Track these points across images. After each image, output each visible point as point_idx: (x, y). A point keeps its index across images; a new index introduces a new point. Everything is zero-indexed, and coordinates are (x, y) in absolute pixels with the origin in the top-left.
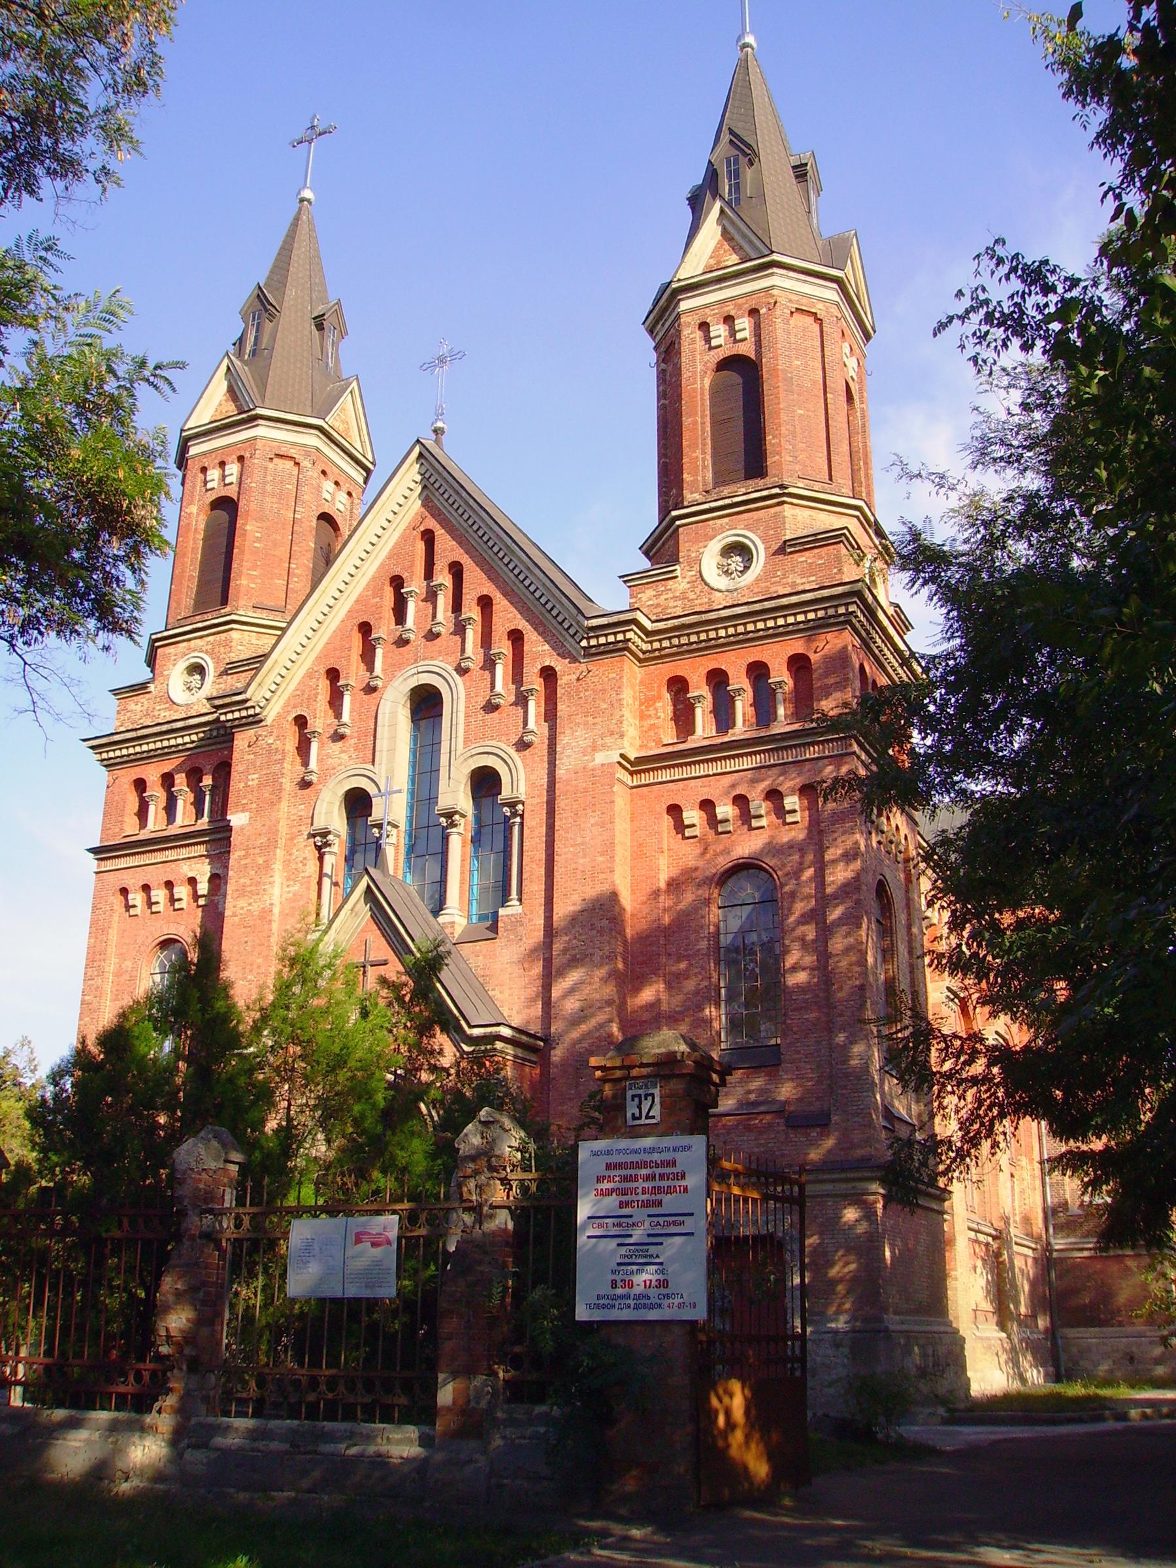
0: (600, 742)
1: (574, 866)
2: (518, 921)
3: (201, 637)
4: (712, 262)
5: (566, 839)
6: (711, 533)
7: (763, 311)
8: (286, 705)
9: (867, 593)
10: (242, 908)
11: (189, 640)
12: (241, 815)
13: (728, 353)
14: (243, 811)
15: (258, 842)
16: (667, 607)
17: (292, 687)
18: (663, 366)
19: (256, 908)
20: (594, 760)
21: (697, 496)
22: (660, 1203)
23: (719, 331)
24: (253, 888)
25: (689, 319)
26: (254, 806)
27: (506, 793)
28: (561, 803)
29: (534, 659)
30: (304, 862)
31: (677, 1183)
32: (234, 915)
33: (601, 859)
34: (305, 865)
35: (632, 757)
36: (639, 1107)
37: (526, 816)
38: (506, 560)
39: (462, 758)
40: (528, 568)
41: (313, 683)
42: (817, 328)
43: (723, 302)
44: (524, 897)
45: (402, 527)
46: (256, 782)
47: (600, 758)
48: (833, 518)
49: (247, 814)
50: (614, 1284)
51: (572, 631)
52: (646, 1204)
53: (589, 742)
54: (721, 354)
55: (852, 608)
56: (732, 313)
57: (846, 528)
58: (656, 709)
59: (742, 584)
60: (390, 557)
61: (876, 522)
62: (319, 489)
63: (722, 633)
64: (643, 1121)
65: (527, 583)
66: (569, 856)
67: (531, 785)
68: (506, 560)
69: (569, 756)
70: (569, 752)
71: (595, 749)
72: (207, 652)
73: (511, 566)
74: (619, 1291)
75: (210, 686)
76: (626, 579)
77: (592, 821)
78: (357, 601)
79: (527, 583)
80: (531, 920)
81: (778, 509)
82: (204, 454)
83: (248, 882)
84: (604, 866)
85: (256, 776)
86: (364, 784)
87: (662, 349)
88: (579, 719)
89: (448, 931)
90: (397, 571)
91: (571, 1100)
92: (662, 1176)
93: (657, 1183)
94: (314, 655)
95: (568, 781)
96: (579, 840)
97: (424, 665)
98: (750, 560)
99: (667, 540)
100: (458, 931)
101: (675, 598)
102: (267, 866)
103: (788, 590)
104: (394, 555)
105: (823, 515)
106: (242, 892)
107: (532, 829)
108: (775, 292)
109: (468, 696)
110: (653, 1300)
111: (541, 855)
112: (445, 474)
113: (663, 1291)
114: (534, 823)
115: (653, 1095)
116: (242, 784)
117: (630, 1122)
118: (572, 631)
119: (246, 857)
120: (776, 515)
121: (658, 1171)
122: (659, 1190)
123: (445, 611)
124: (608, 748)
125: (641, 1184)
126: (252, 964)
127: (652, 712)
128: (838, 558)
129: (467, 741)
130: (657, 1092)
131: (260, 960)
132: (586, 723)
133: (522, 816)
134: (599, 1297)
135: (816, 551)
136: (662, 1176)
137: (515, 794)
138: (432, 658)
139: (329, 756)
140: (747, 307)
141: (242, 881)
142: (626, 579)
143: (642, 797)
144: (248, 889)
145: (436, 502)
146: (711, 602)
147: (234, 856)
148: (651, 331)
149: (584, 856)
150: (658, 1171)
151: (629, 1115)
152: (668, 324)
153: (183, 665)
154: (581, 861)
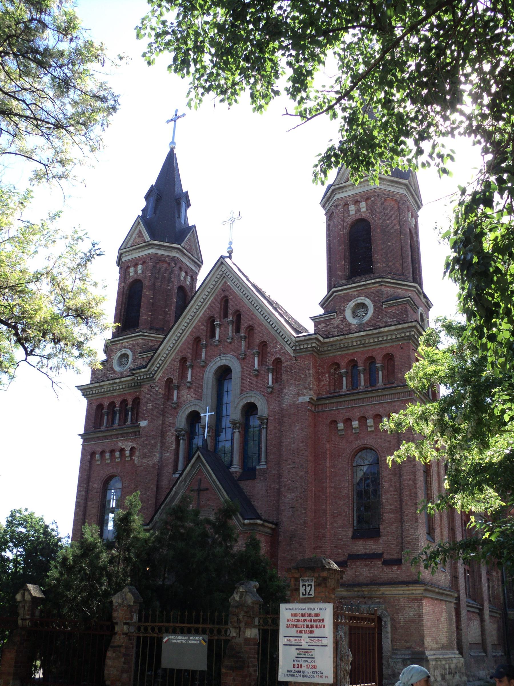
2: (264, 471)
3: (127, 342)
6: (350, 298)
8: (162, 374)
9: (419, 327)
11: (122, 343)
13: (357, 218)
14: (145, 420)
16: (330, 332)
17: (166, 366)
18: (329, 222)
19: (150, 463)
21: (344, 281)
22: (313, 632)
27: (259, 413)
29: (272, 355)
31: (320, 623)
33: (301, 445)
35: (315, 399)
36: (305, 590)
38: (260, 310)
41: (175, 363)
42: (396, 206)
43: (354, 195)
45: (214, 295)
47: (301, 399)
48: (404, 292)
50: (294, 666)
51: (288, 343)
52: (308, 632)
53: (296, 392)
54: (355, 218)
55: (413, 333)
56: (359, 200)
57: (409, 297)
59: (364, 322)
60: (208, 308)
61: (423, 293)
62: (179, 275)
63: (355, 344)
64: (307, 596)
65: (269, 321)
68: (260, 310)
70: (287, 396)
71: (298, 395)
72: (129, 348)
73: (262, 313)
74: (296, 669)
75: (130, 364)
76: (313, 319)
78: (194, 327)
79: (269, 321)
80: (270, 471)
81: (379, 288)
82: (129, 261)
86: (197, 409)
87: (329, 215)
89: (234, 475)
92: (314, 621)
93: (312, 623)
94: (176, 351)
96: (292, 436)
97: (224, 357)
98: (367, 310)
99: (331, 301)
100: (238, 475)
101: (334, 328)
102: (156, 443)
103: (384, 324)
104: (211, 307)
108: (377, 190)
109: (243, 371)
110: (311, 674)
113: (314, 670)
114: (272, 428)
115: (311, 585)
117: (301, 596)
118: (288, 343)
119: (146, 440)
120: (378, 291)
121: (313, 618)
122: (313, 626)
123: (232, 333)
124: (305, 395)
125: (306, 623)
127: (324, 379)
128: (407, 311)
129: (242, 391)
130: (313, 584)
133: (267, 424)
134: (288, 671)
135: (396, 307)
136: (314, 621)
138: (227, 354)
139: (182, 396)
142: (313, 319)
146: (350, 329)
148: (324, 206)
149: (294, 443)
150: (313, 618)
151: (301, 594)
152: (331, 204)
153: (119, 354)
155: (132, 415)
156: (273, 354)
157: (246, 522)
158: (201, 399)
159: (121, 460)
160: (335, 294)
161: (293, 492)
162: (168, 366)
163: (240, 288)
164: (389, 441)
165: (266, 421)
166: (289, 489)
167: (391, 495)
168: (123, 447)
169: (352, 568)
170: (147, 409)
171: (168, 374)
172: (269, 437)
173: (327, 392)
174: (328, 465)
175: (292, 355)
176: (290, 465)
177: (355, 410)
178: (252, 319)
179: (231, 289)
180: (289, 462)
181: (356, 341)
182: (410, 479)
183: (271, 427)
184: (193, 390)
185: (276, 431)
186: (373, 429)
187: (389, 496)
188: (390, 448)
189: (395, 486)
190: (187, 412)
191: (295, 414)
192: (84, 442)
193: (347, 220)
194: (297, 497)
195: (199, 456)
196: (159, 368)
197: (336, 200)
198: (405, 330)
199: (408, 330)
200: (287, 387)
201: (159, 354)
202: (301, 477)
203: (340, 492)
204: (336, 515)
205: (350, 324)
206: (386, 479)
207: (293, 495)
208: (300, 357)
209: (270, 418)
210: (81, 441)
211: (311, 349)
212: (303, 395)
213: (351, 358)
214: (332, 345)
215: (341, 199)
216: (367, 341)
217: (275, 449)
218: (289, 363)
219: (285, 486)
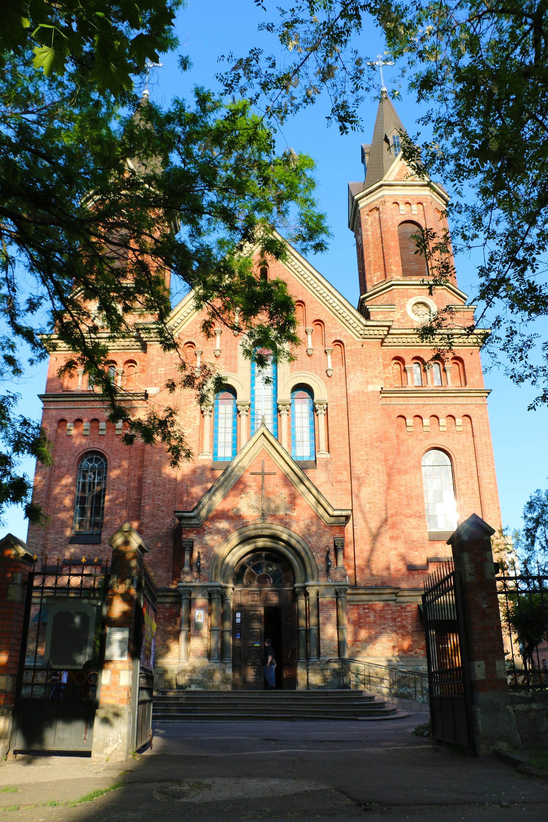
0: (370, 380)
4: (398, 177)
5: (355, 424)
7: (425, 204)
14: (155, 386)
21: (399, 277)
23: (402, 207)
28: (352, 406)
30: (194, 418)
39: (290, 378)
46: (163, 372)
47: (371, 388)
66: (358, 433)
67: (332, 396)
70: (353, 382)
71: (367, 383)
85: (163, 369)
88: (358, 368)
96: (363, 425)
105: (455, 299)
107: (333, 417)
111: (229, 438)
114: (334, 415)
116: (153, 373)
124: (375, 384)
127: (387, 371)
132: (362, 370)
140: (417, 201)
154: (364, 436)
156: (331, 335)
158: (235, 371)
159: (107, 433)
162: (187, 328)
165: (325, 406)
170: (156, 373)
173: (391, 385)
175: (357, 339)
176: (362, 456)
177: (427, 408)
178: (302, 294)
180: (362, 453)
182: (491, 483)
185: (340, 418)
186: (445, 429)
189: (473, 489)
191: (364, 402)
192: (45, 405)
193: (397, 218)
194: (374, 492)
197: (383, 196)
200: (352, 373)
203: (412, 490)
205: (412, 321)
208: (368, 344)
210: (42, 405)
212: (373, 383)
215: (391, 196)
217: (340, 439)
218: (353, 347)
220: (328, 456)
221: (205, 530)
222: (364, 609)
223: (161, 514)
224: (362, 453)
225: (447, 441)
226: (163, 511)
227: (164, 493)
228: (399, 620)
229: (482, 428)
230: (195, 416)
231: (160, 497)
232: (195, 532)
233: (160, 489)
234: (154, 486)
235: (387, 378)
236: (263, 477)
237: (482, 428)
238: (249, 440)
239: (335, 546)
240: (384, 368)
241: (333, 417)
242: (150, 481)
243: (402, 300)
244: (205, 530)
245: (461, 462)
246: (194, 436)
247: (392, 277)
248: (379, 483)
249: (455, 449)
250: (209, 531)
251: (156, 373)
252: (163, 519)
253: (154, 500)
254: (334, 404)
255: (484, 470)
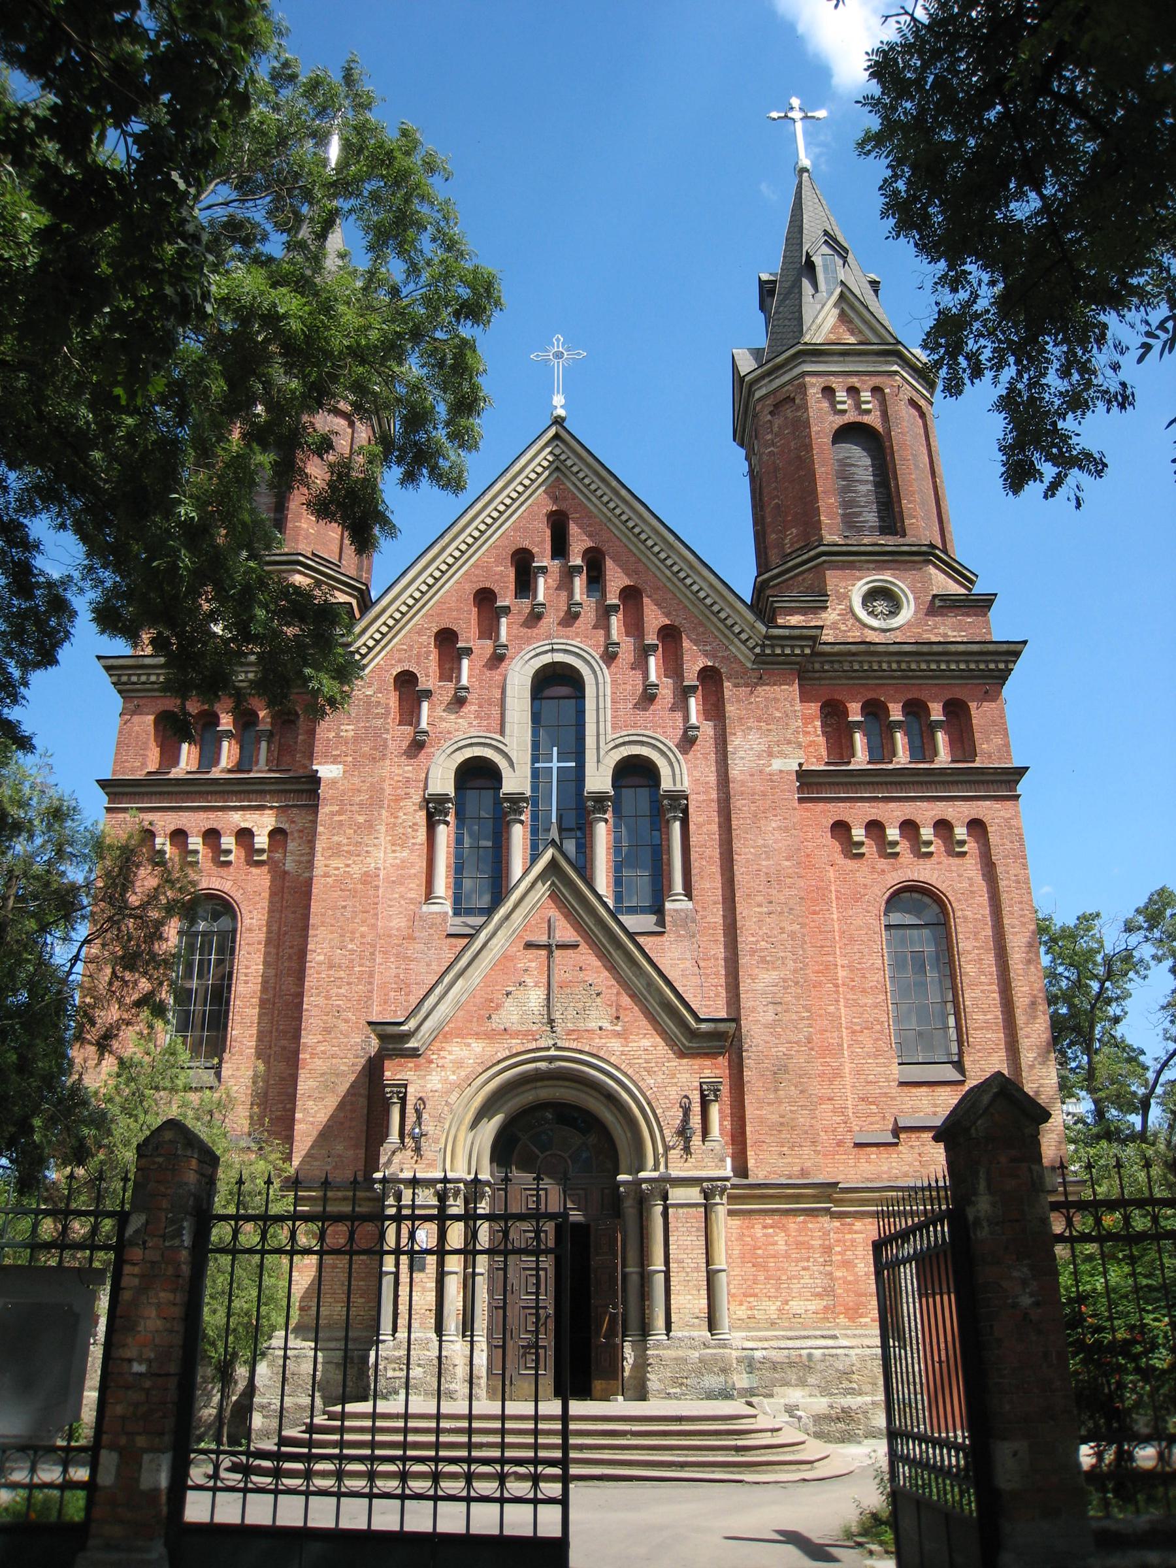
0: (776, 749)
1: (755, 867)
4: (832, 337)
7: (887, 391)
10: (337, 869)
12: (333, 767)
13: (852, 419)
14: (333, 763)
15: (357, 799)
19: (356, 870)
20: (770, 765)
24: (351, 848)
25: (813, 380)
26: (350, 759)
27: (666, 784)
28: (737, 803)
32: (326, 875)
33: (787, 863)
34: (417, 831)
37: (691, 810)
39: (612, 745)
40: (691, 567)
41: (424, 639)
44: (694, 893)
47: (777, 764)
48: (957, 586)
49: (341, 767)
51: (744, 636)
56: (857, 385)
58: (815, 727)
63: (885, 666)
69: (742, 758)
70: (742, 754)
71: (771, 755)
77: (774, 825)
83: (345, 841)
84: (790, 871)
85: (351, 727)
90: (526, 544)
91: (769, 1104)
95: (743, 783)
96: (760, 842)
102: (370, 826)
106: (336, 851)
109: (614, 682)
112: (590, 460)
114: (701, 819)
116: (332, 735)
118: (744, 636)
119: (339, 813)
126: (353, 933)
127: (810, 729)
131: (363, 929)
137: (679, 787)
141: (336, 838)
143: (807, 810)
144: (345, 848)
145: (569, 485)
147: (324, 811)
149: (768, 858)
154: (764, 863)
155: (269, 750)
157: (703, 1026)
160: (824, 558)
161: (774, 969)
163: (605, 499)
164: (969, 879)
166: (763, 960)
167: (983, 991)
168: (244, 825)
169: (911, 1147)
170: (338, 736)
171: (400, 661)
172: (693, 840)
174: (835, 917)
175: (749, 665)
176: (760, 906)
179: (574, 497)
180: (759, 899)
181: (889, 663)
183: (694, 818)
184: (474, 708)
187: (977, 993)
188: (971, 892)
190: (460, 757)
194: (785, 981)
195: (553, 859)
196: (378, 642)
198: (997, 658)
199: (1004, 658)
201: (384, 611)
202: (792, 936)
204: (858, 1028)
206: (970, 957)
207: (774, 975)
209: (691, 797)
211: (799, 659)
213: (871, 695)
214: (832, 662)
216: (913, 666)
219: (753, 952)
220: (690, 905)
221: (431, 1062)
222: (765, 1227)
223: (343, 1026)
224: (759, 899)
225: (935, 876)
226: (346, 1021)
227: (349, 984)
228: (838, 1249)
229: (1009, 846)
230: (415, 824)
231: (342, 991)
232: (410, 1065)
233: (342, 974)
234: (331, 967)
235: (811, 744)
236: (551, 953)
237: (1009, 846)
238: (526, 873)
239: (703, 1097)
240: (805, 724)
241: (699, 826)
242: (321, 958)
243: (843, 584)
244: (431, 1062)
245: (965, 918)
246: (413, 865)
247: (821, 538)
248: (795, 961)
249: (954, 890)
250: (441, 1062)
251: (338, 736)
252: (346, 1036)
253: (328, 998)
254: (702, 797)
255: (1015, 934)
